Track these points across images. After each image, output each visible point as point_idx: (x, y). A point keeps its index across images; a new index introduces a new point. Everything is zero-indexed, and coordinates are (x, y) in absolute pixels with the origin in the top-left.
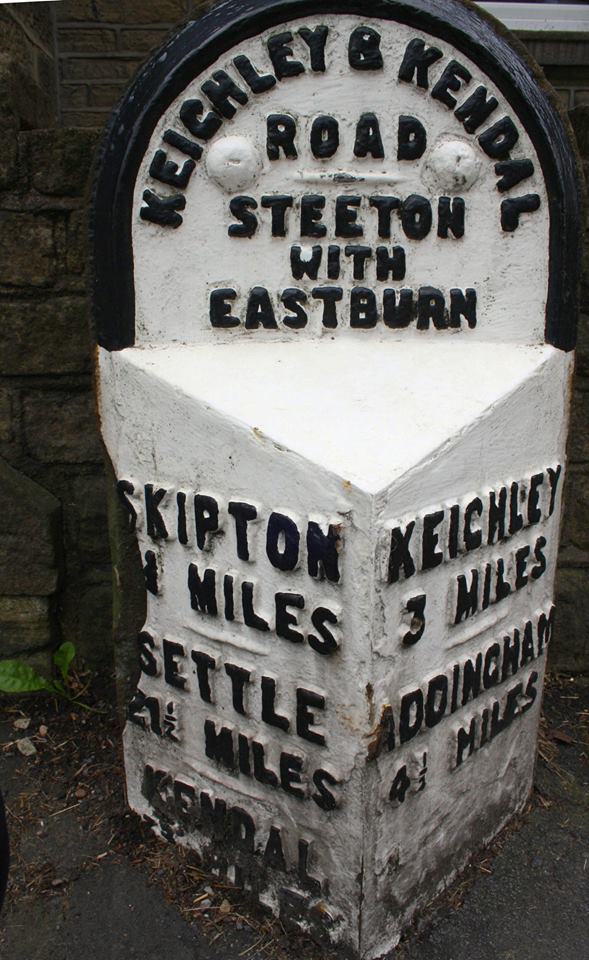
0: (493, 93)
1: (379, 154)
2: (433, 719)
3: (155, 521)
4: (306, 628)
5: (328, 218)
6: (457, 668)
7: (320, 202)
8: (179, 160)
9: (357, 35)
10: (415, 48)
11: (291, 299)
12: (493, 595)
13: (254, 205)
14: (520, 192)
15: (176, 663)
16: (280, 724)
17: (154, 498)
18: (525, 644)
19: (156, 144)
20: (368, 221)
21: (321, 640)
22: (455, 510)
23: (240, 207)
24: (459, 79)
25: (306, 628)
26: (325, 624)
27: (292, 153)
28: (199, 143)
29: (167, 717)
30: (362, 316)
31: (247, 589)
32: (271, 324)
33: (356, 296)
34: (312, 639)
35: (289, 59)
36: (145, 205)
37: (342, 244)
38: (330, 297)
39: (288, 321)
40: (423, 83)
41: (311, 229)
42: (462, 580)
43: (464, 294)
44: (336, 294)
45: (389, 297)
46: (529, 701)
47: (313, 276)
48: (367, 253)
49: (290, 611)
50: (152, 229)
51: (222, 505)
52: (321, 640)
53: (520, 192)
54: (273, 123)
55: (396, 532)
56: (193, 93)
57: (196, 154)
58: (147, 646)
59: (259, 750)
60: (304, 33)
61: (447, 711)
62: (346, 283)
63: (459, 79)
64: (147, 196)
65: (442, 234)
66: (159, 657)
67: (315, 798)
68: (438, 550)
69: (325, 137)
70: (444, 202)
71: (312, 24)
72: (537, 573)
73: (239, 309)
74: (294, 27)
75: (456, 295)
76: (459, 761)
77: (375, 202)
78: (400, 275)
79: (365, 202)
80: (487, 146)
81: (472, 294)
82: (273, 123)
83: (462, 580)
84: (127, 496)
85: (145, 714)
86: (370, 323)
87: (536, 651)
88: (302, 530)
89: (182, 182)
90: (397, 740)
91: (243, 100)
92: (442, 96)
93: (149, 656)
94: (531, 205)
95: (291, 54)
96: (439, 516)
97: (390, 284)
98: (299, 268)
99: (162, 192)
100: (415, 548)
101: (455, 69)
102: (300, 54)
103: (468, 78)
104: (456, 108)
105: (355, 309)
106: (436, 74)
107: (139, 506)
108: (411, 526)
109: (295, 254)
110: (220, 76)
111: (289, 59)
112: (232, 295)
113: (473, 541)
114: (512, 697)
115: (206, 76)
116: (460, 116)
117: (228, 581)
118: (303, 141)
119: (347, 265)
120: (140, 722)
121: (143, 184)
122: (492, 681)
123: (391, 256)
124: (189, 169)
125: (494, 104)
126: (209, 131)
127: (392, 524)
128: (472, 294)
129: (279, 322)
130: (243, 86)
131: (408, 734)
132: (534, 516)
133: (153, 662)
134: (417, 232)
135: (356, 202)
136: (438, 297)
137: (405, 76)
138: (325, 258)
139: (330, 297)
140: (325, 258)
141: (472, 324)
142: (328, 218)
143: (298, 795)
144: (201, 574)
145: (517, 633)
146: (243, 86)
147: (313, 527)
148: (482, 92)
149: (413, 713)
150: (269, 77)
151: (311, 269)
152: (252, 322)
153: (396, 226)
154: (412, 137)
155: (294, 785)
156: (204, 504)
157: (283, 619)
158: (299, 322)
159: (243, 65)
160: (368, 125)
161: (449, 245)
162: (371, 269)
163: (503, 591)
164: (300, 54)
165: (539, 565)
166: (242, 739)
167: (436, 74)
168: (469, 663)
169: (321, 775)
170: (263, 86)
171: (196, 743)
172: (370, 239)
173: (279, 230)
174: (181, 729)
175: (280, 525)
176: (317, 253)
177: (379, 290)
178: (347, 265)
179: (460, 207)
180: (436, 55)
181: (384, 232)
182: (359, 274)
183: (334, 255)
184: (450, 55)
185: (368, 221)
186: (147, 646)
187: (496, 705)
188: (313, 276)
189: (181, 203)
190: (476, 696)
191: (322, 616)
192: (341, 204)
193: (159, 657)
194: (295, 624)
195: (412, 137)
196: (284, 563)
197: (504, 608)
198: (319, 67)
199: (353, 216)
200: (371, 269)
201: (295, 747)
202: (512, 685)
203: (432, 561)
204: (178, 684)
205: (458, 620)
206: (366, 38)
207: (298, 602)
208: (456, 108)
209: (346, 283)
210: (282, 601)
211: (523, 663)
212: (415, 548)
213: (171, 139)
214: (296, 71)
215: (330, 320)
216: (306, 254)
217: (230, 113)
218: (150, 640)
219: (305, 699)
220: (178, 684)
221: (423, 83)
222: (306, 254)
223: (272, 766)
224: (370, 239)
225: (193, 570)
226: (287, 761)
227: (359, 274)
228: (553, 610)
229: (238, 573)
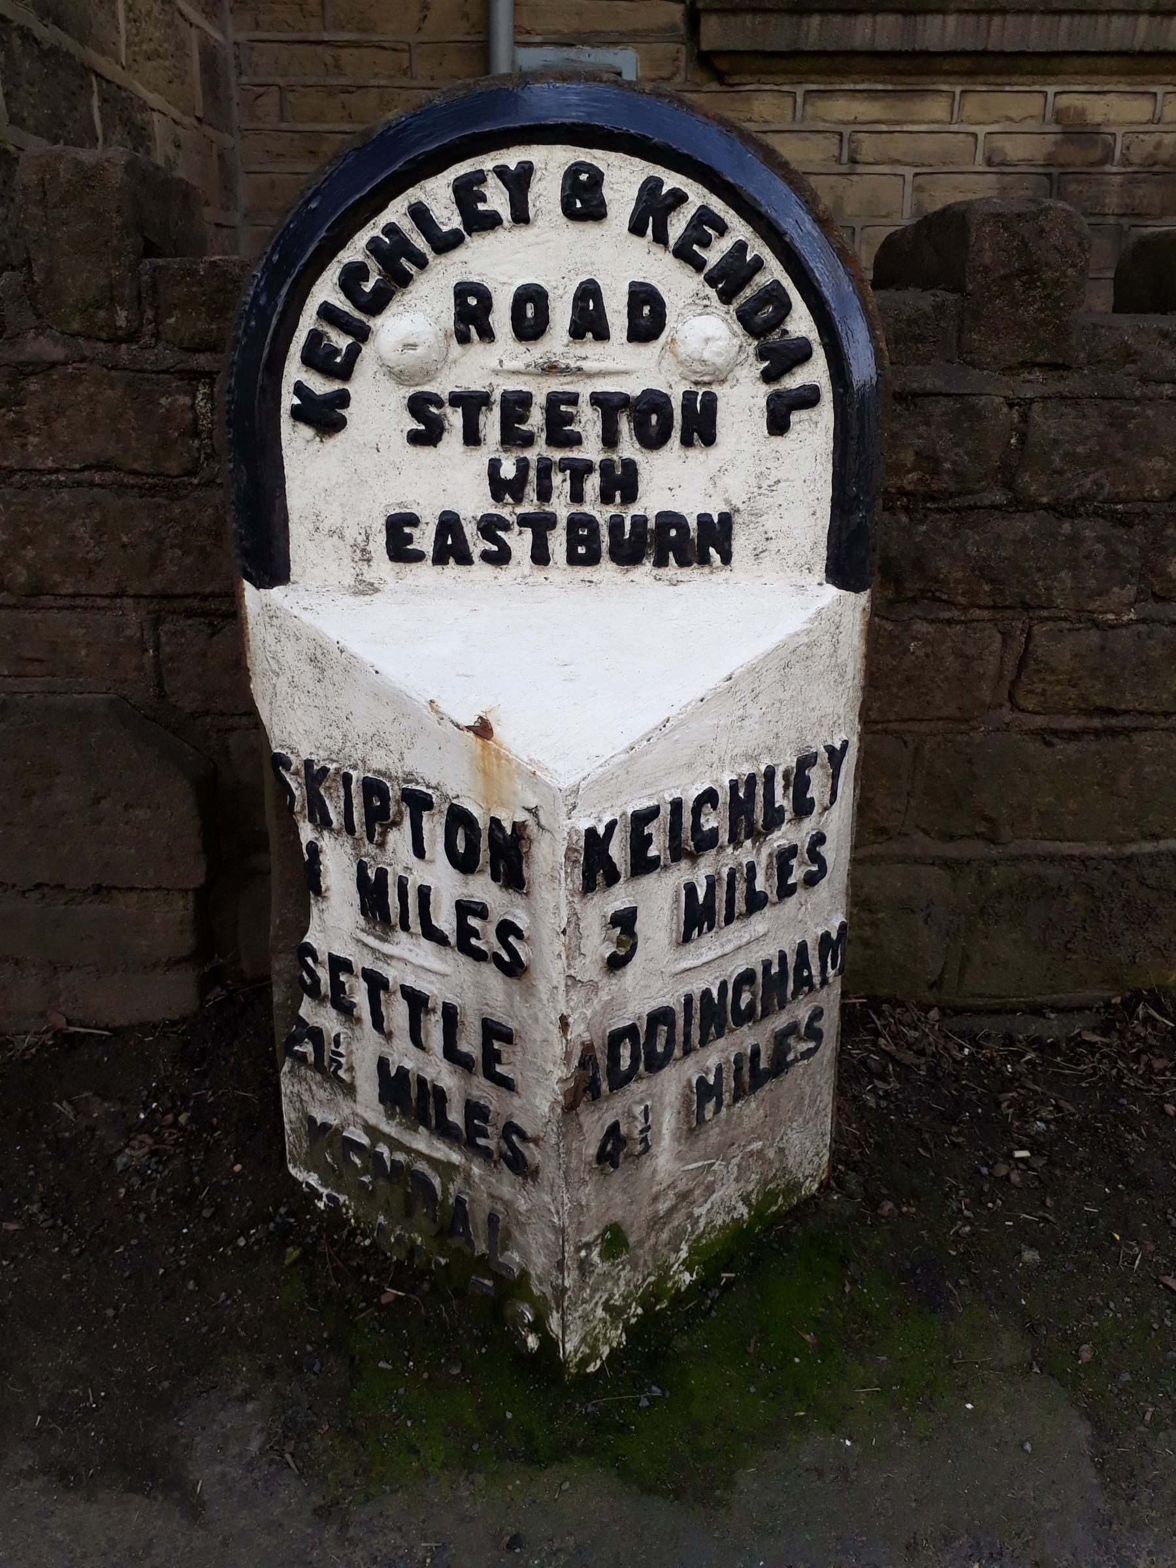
0: (758, 248)
1: (602, 335)
2: (656, 1064)
5: (536, 419)
6: (689, 999)
8: (342, 342)
9: (572, 173)
10: (651, 187)
11: (490, 526)
12: (740, 906)
13: (439, 403)
15: (343, 984)
19: (308, 321)
20: (589, 423)
21: (507, 958)
22: (677, 805)
23: (419, 405)
24: (710, 231)
25: (488, 941)
26: (511, 939)
27: (487, 335)
29: (334, 1053)
30: (581, 550)
31: (424, 893)
32: (464, 559)
33: (574, 523)
34: (497, 959)
35: (481, 207)
36: (297, 401)
37: (557, 455)
38: (540, 525)
39: (487, 557)
41: (513, 437)
42: (691, 889)
43: (716, 520)
45: (616, 524)
46: (812, 1045)
48: (588, 467)
49: (473, 922)
50: (306, 432)
52: (507, 958)
55: (591, 833)
56: (355, 251)
57: (362, 334)
58: (309, 960)
59: (440, 1095)
60: (501, 172)
61: (677, 1052)
62: (561, 507)
63: (710, 231)
64: (300, 389)
65: (687, 442)
66: (324, 974)
67: (503, 1156)
68: (653, 852)
69: (530, 311)
70: (689, 397)
71: (511, 158)
72: (811, 880)
73: (424, 539)
74: (488, 162)
75: (704, 520)
76: (701, 1120)
77: (597, 400)
78: (630, 496)
79: (584, 399)
80: (745, 318)
81: (726, 520)
82: (463, 291)
83: (691, 889)
84: (283, 772)
85: (307, 1048)
86: (592, 559)
87: (817, 980)
88: (483, 823)
89: (345, 372)
90: (605, 1086)
92: (685, 254)
93: (312, 973)
94: (808, 398)
95: (483, 199)
96: (652, 814)
98: (499, 488)
99: (321, 386)
100: (618, 851)
101: (705, 216)
102: (497, 199)
103: (722, 229)
104: (706, 270)
105: (573, 541)
106: (677, 226)
108: (611, 826)
109: (494, 465)
111: (481, 207)
112: (413, 520)
113: (706, 841)
114: (781, 1039)
116: (711, 280)
117: (402, 884)
118: (501, 318)
119: (560, 482)
120: (301, 1058)
121: (294, 371)
122: (744, 1017)
123: (619, 472)
124: (353, 353)
126: (377, 304)
129: (476, 553)
130: (420, 243)
131: (620, 1081)
132: (803, 808)
133: (316, 981)
134: (653, 440)
135: (573, 399)
137: (636, 228)
138: (532, 474)
139: (540, 525)
140: (532, 474)
141: (726, 559)
142: (536, 419)
143: (486, 1153)
144: (371, 874)
145: (783, 956)
146: (420, 243)
147: (495, 822)
149: (625, 1052)
150: (455, 232)
152: (440, 559)
154: (646, 310)
155: (481, 1141)
157: (465, 933)
158: (500, 557)
159: (419, 213)
160: (589, 293)
161: (697, 454)
162: (592, 484)
163: (756, 902)
164: (497, 199)
165: (815, 868)
166: (421, 1081)
167: (677, 226)
168: (706, 993)
169: (510, 1129)
170: (446, 243)
171: (368, 1087)
173: (472, 437)
174: (351, 1069)
175: (458, 818)
176: (522, 466)
177: (603, 514)
178: (560, 482)
179: (711, 401)
180: (678, 198)
181: (610, 439)
182: (577, 496)
183: (545, 469)
184: (697, 196)
185: (589, 423)
186: (309, 960)
187: (756, 1052)
189: (343, 399)
190: (720, 1035)
191: (507, 929)
193: (324, 974)
194: (478, 938)
195: (646, 310)
196: (464, 864)
197: (759, 923)
198: (521, 217)
199: (570, 419)
200: (592, 484)
201: (483, 1090)
202: (780, 1021)
203: (642, 865)
206: (584, 177)
207: (481, 911)
208: (706, 270)
210: (464, 909)
211: (795, 995)
212: (618, 851)
213: (327, 313)
214: (491, 222)
215: (540, 556)
216: (508, 470)
217: (405, 280)
218: (312, 953)
219: (493, 1031)
220: (346, 1009)
221: (661, 238)
222: (508, 470)
223: (456, 1116)
224: (592, 450)
225: (362, 868)
226: (474, 1110)
227: (577, 496)
228: (843, 927)
229: (420, 875)
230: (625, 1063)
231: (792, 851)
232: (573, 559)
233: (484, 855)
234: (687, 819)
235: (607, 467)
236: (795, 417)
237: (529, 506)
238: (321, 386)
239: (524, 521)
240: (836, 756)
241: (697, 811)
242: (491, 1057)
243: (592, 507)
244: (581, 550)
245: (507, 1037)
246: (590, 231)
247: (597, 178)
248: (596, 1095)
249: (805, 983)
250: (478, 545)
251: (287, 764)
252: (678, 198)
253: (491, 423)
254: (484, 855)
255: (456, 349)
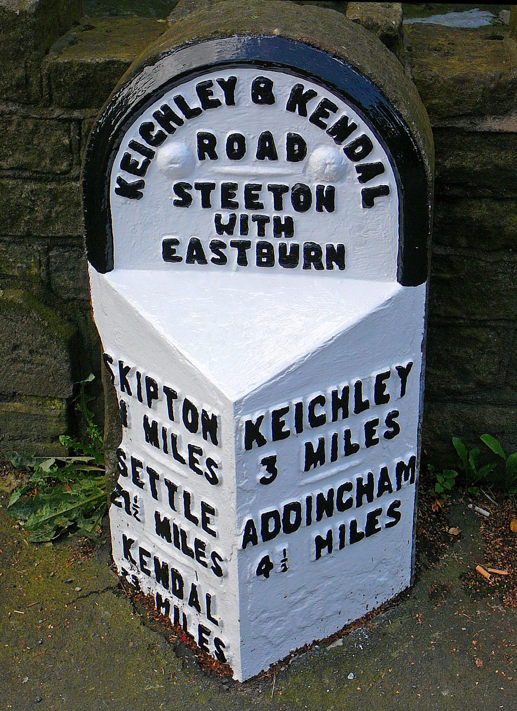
0: (354, 118)
1: (274, 157)
3: (124, 383)
4: (203, 467)
5: (240, 198)
6: (309, 500)
7: (234, 187)
8: (141, 159)
9: (256, 85)
10: (297, 91)
11: (216, 247)
12: (341, 451)
14: (375, 183)
15: (138, 472)
16: (194, 520)
17: (124, 371)
18: (381, 482)
19: (124, 149)
21: (211, 476)
22: (299, 406)
23: (179, 189)
24: (328, 111)
25: (203, 467)
26: (212, 467)
27: (214, 156)
28: (153, 148)
29: (134, 505)
30: (264, 260)
31: (174, 439)
32: (202, 260)
33: (260, 246)
34: (207, 475)
35: (210, 98)
36: (118, 186)
37: (250, 213)
39: (214, 260)
40: (303, 113)
42: (309, 446)
43: (336, 248)
44: (248, 244)
45: (282, 248)
46: (393, 520)
47: (230, 233)
48: (267, 220)
49: (196, 456)
50: (122, 199)
51: (160, 387)
52: (211, 476)
53: (375, 183)
54: (201, 137)
57: (150, 155)
58: (122, 457)
60: (221, 82)
62: (254, 239)
63: (328, 111)
64: (120, 181)
65: (319, 209)
66: (129, 465)
67: (212, 567)
68: (285, 429)
69: (236, 146)
70: (320, 189)
71: (226, 75)
73: (182, 251)
75: (330, 249)
77: (271, 188)
78: (290, 233)
79: (265, 188)
80: (349, 152)
81: (341, 248)
82: (201, 137)
83: (309, 446)
84: (109, 364)
85: (121, 500)
86: (270, 263)
87: (394, 486)
88: (200, 412)
89: (142, 172)
90: (260, 539)
91: (180, 122)
93: (123, 464)
94: (384, 191)
95: (212, 94)
96: (285, 411)
97: (283, 240)
98: (220, 229)
99: (131, 179)
103: (335, 109)
104: (327, 129)
106: (312, 107)
107: (116, 371)
109: (218, 218)
110: (165, 108)
111: (210, 98)
112: (176, 242)
115: (157, 107)
117: (164, 431)
118: (221, 149)
119: (253, 227)
120: (119, 505)
122: (344, 507)
123: (283, 222)
124: (146, 164)
125: (354, 127)
126: (160, 139)
127: (246, 418)
128: (341, 248)
130: (180, 114)
133: (126, 468)
135: (259, 188)
136: (317, 249)
137: (290, 108)
141: (342, 267)
142: (240, 198)
144: (150, 422)
145: (370, 477)
146: (180, 114)
147: (204, 412)
148: (345, 119)
150: (198, 109)
151: (229, 229)
152: (190, 260)
153: (287, 199)
154: (296, 147)
155: (201, 558)
156: (150, 382)
157: (193, 461)
158: (222, 260)
159: (180, 101)
162: (270, 228)
164: (219, 94)
165: (392, 430)
166: (175, 526)
167: (312, 107)
168: (320, 496)
169: (214, 555)
170: (192, 114)
172: (270, 212)
173: (206, 204)
174: (143, 514)
175: (188, 406)
176: (233, 219)
177: (276, 243)
178: (253, 227)
179: (331, 191)
180: (312, 94)
181: (278, 206)
182: (261, 232)
183: (244, 220)
186: (122, 457)
188: (230, 233)
189: (141, 184)
191: (210, 463)
192: (248, 189)
193: (129, 465)
194: (198, 464)
195: (296, 147)
196: (192, 428)
197: (355, 460)
198: (230, 101)
199: (257, 197)
200: (270, 228)
202: (372, 508)
204: (141, 485)
205: (307, 469)
207: (200, 452)
208: (327, 129)
209: (254, 239)
210: (192, 449)
211: (379, 495)
213: (134, 145)
214: (216, 104)
215: (242, 261)
216: (225, 220)
218: (124, 455)
219: (206, 508)
220: (141, 485)
221: (303, 113)
222: (225, 220)
223: (191, 545)
224: (270, 212)
225: (146, 419)
228: (413, 459)
230: (271, 530)
231: (375, 422)
232: (260, 263)
233: (200, 426)
234: (306, 412)
235: (277, 220)
236: (376, 200)
237: (237, 237)
238: (131, 179)
239: (233, 244)
240: (403, 373)
241: (311, 408)
242: (206, 521)
243: (270, 237)
244: (264, 260)
245: (212, 512)
246: (266, 109)
247: (269, 84)
248: (255, 543)
249: (384, 488)
250: (210, 255)
251: (111, 361)
252: (312, 94)
253: (216, 197)
254: (200, 426)
255: (199, 163)
